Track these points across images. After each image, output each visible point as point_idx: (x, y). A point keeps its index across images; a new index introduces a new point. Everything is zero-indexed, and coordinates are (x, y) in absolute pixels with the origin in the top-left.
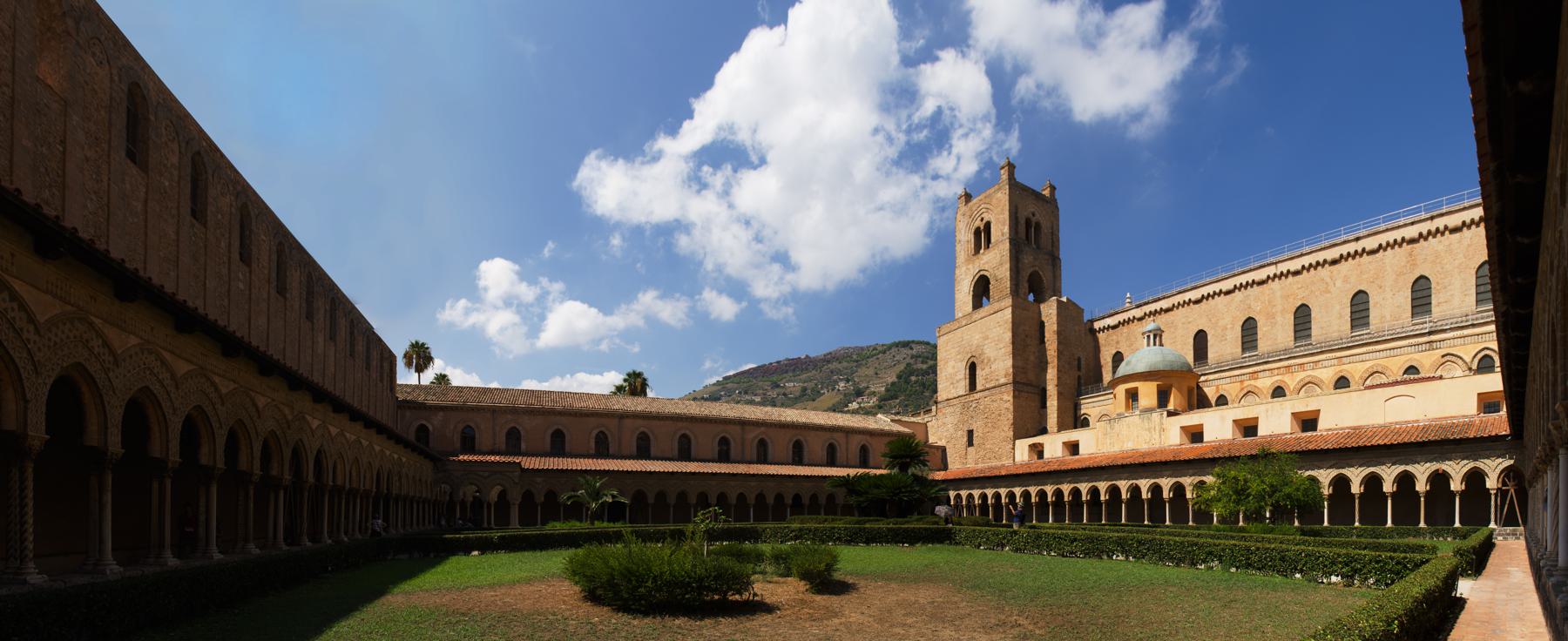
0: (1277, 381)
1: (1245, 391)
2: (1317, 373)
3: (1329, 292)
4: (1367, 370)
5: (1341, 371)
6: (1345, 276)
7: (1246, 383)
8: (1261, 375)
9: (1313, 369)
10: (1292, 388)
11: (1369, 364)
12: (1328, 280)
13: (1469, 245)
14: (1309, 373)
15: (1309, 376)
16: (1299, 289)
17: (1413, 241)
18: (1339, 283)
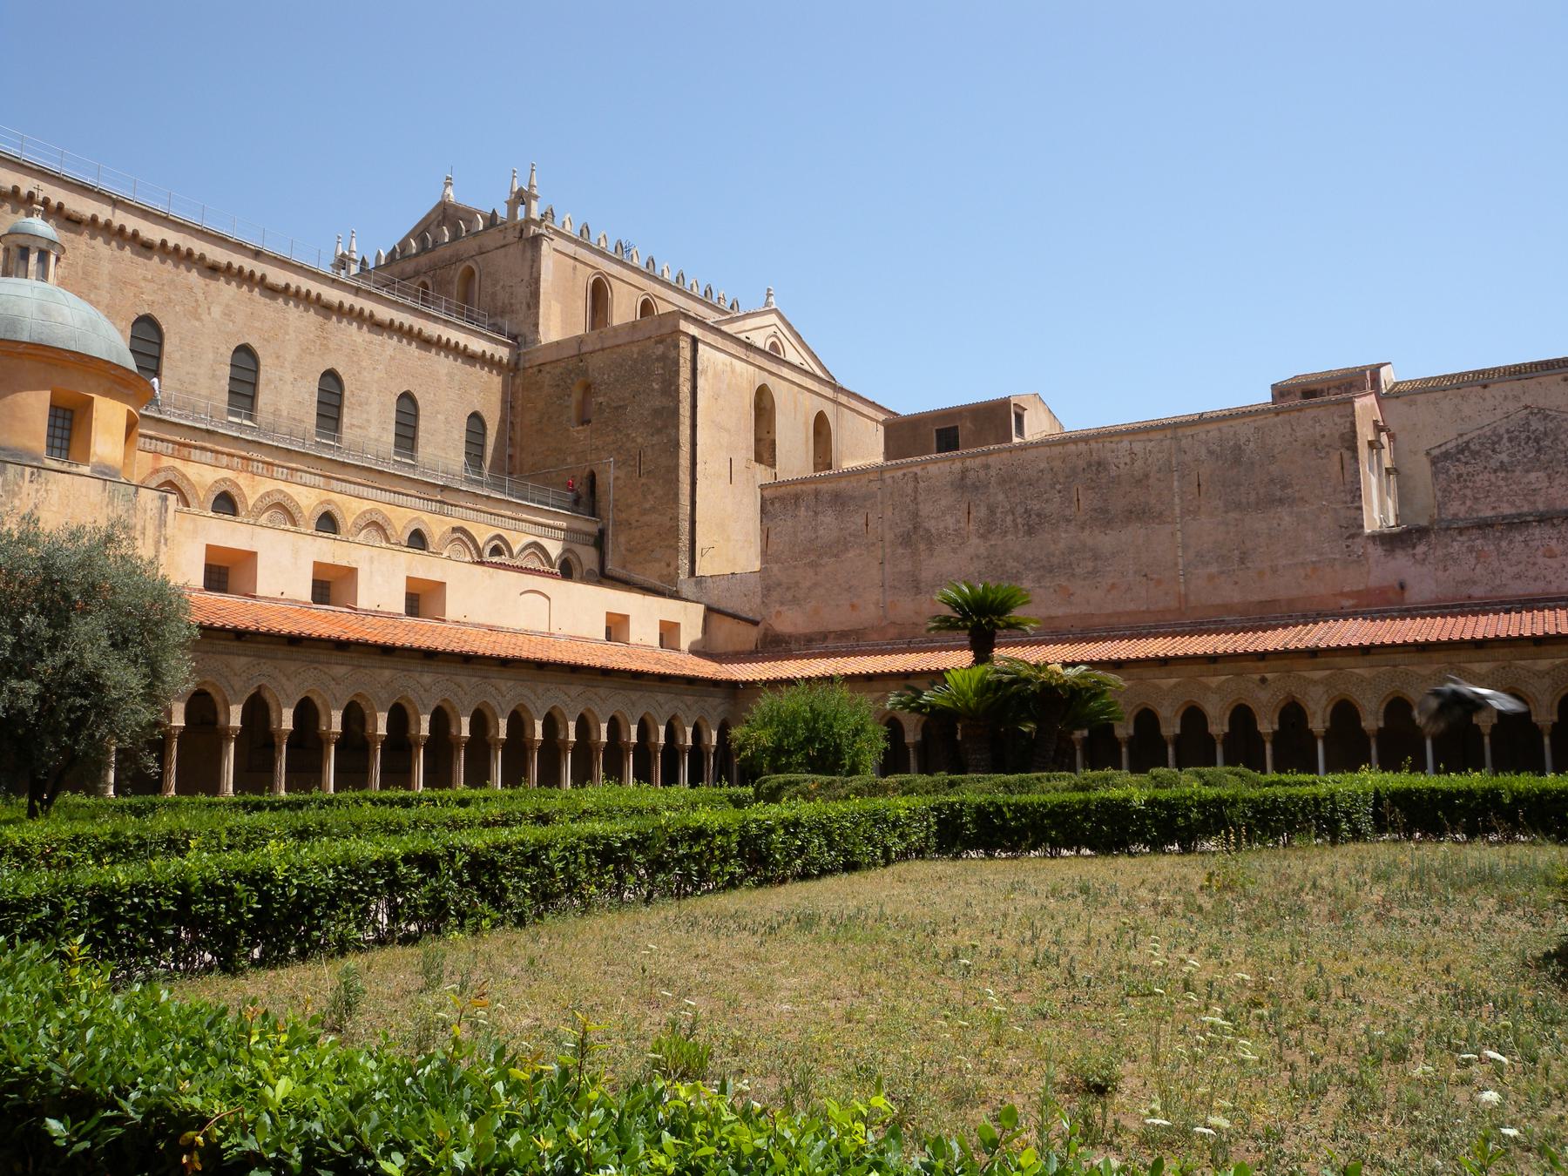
0: (224, 480)
1: (161, 478)
2: (293, 490)
3: (199, 319)
4: (364, 512)
5: (329, 502)
6: (227, 306)
7: (166, 462)
8: (196, 454)
9: (285, 481)
10: (251, 503)
11: (367, 505)
12: (201, 297)
13: (392, 358)
14: (282, 486)
15: (281, 492)
16: (145, 279)
17: (327, 309)
18: (216, 311)
